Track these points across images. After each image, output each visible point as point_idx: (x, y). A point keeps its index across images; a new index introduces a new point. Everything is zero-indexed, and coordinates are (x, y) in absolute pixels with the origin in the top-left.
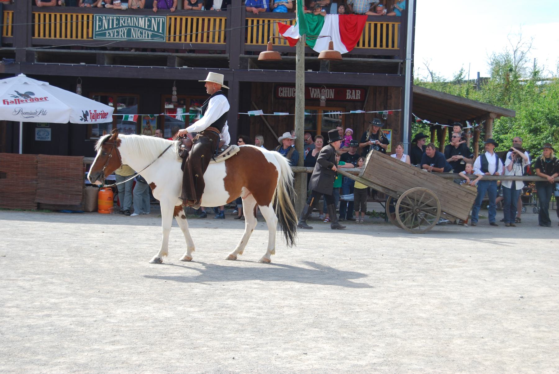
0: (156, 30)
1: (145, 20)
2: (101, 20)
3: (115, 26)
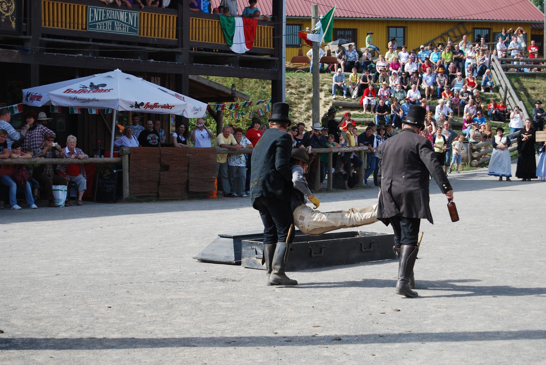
0: (132, 25)
1: (124, 13)
2: (93, 12)
3: (103, 19)
